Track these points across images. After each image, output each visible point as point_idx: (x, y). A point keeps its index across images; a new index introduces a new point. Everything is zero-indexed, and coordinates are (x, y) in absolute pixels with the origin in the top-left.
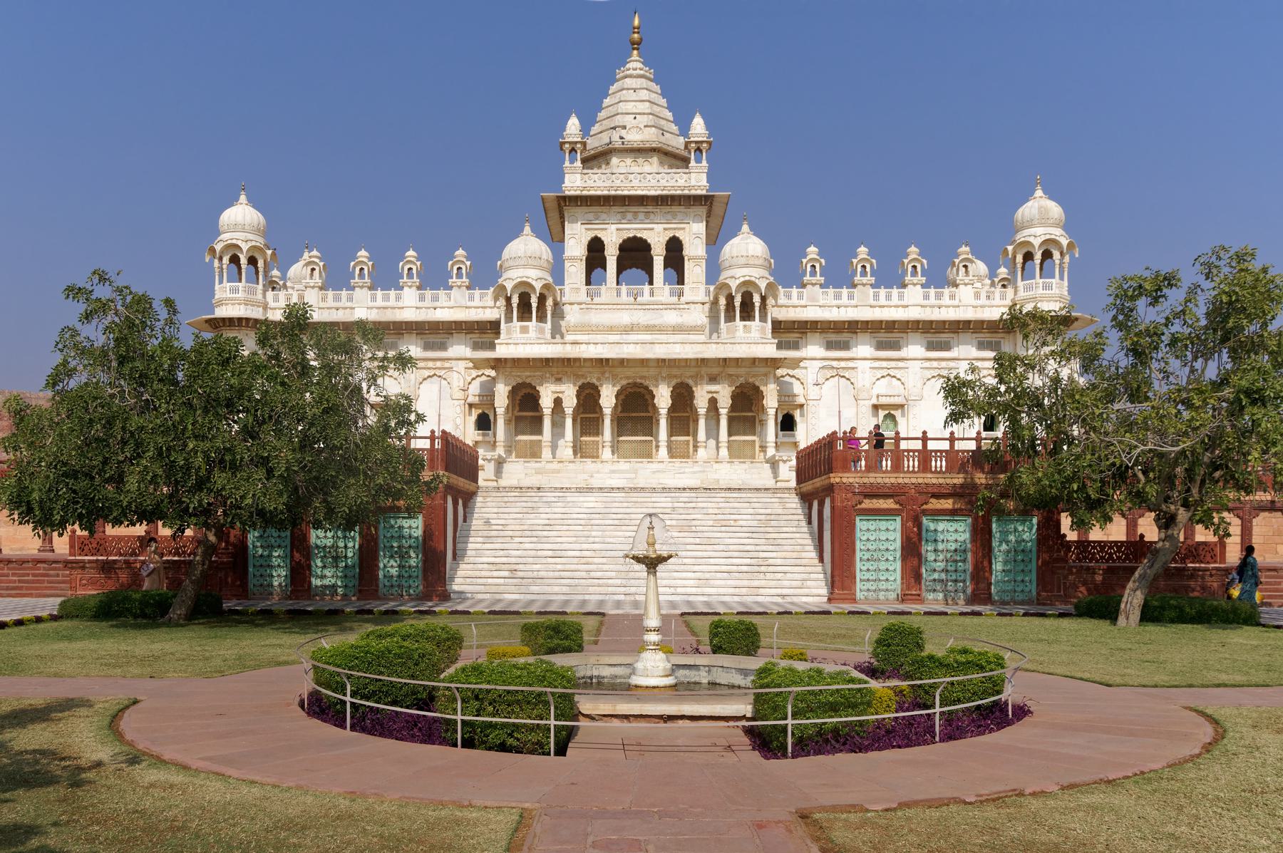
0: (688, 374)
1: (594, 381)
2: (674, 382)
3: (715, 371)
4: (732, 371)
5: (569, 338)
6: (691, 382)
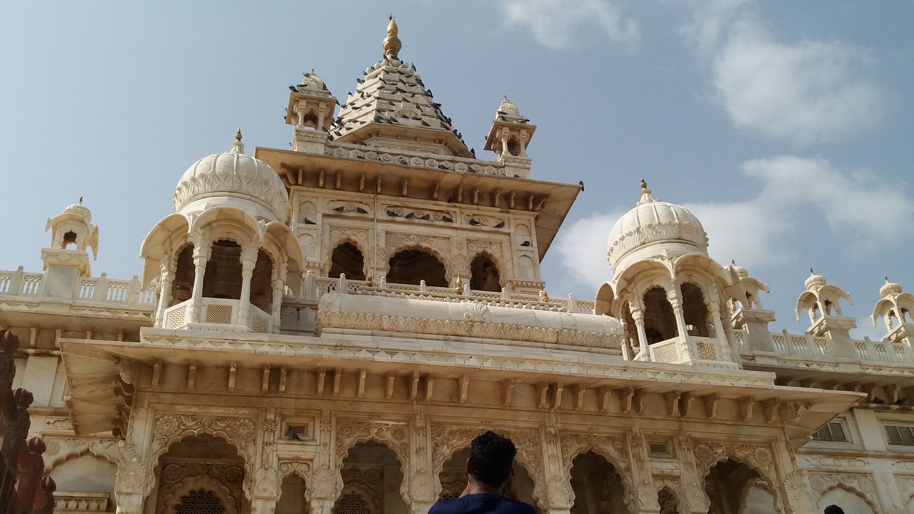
0: (605, 431)
1: (388, 436)
2: (574, 449)
3: (664, 427)
4: (698, 431)
5: (327, 337)
6: (611, 452)
